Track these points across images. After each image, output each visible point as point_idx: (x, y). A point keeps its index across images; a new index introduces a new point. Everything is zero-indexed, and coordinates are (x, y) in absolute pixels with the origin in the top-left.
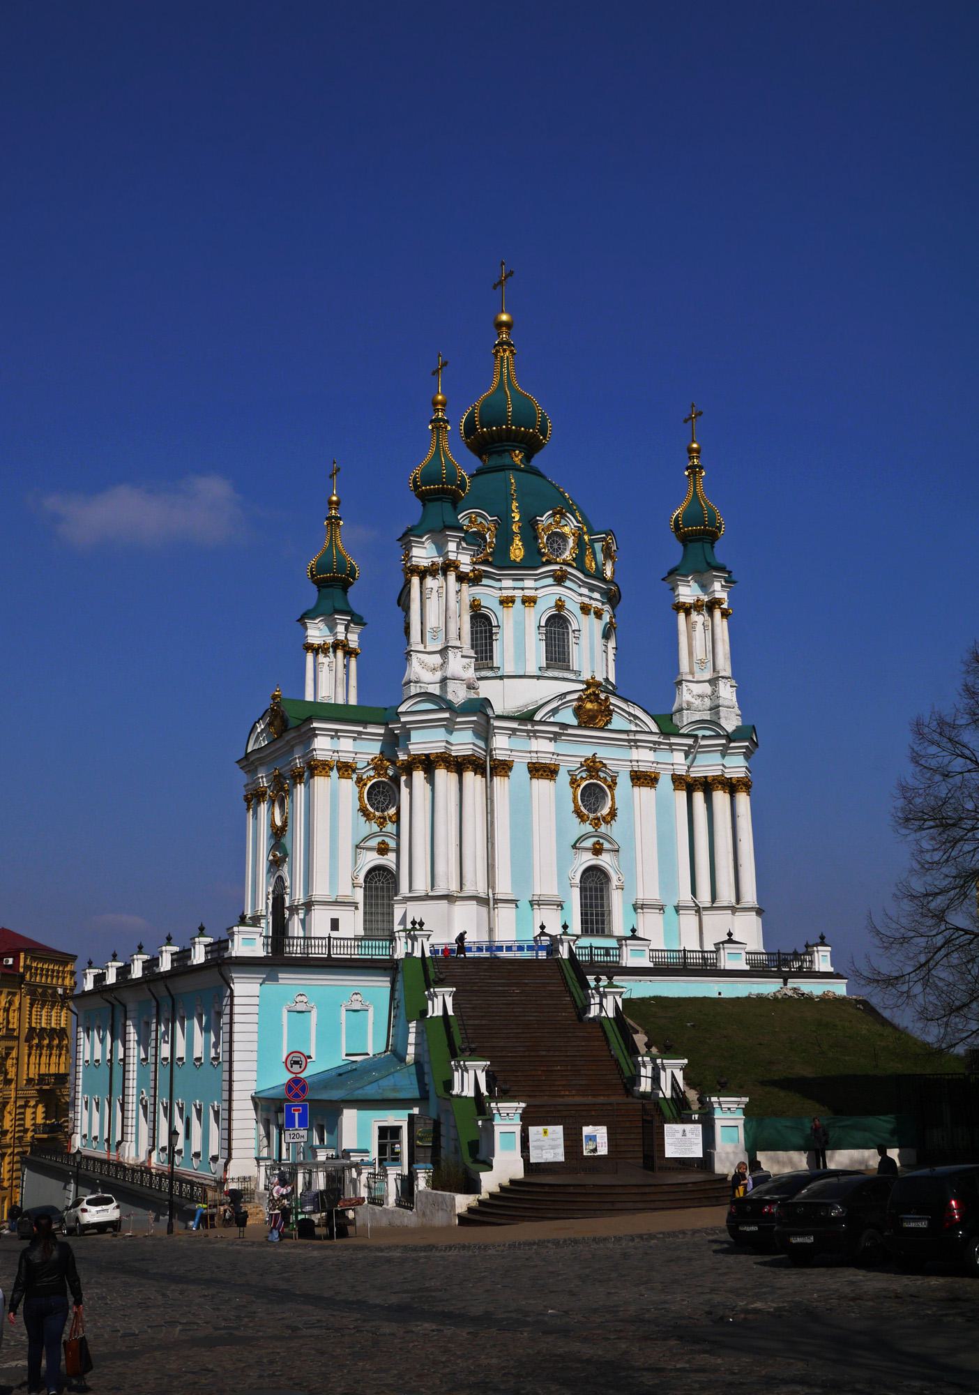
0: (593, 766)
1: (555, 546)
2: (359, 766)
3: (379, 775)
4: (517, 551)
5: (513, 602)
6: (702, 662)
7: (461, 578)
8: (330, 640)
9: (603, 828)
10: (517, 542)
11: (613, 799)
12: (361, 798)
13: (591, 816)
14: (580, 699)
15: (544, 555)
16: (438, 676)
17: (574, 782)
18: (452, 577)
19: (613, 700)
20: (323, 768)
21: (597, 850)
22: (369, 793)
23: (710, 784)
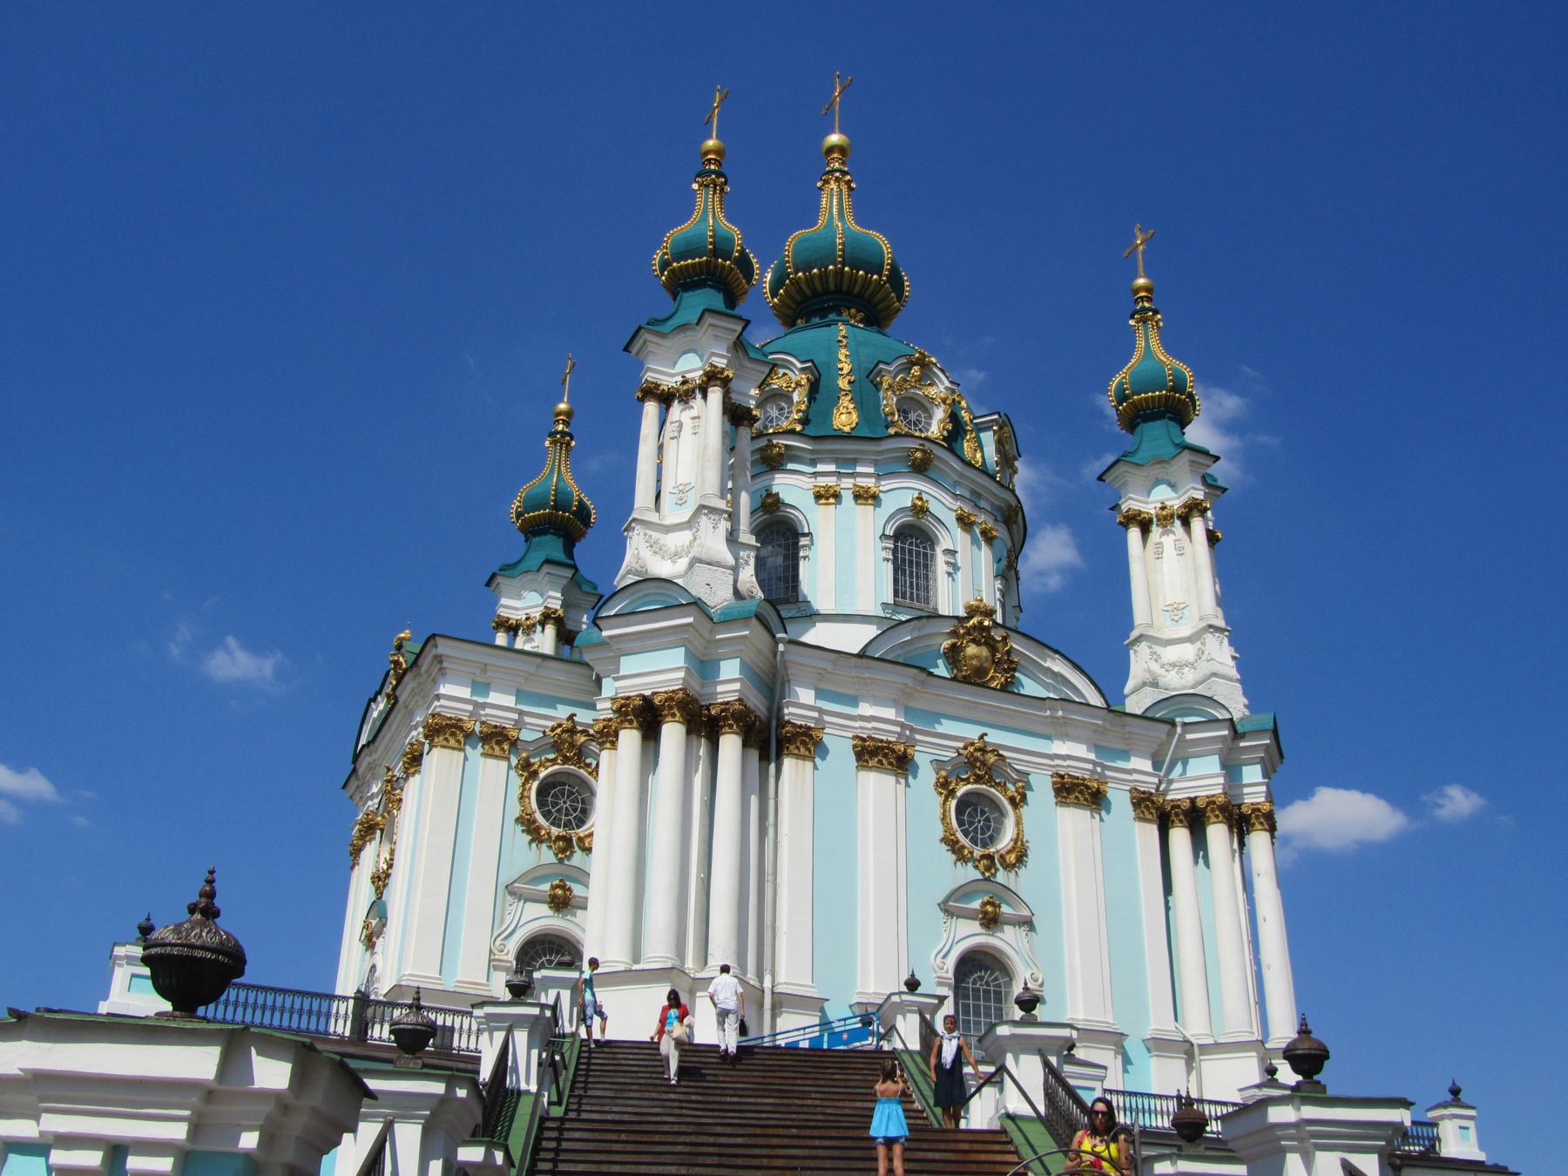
0: (979, 763)
1: (912, 416)
2: (526, 735)
3: (566, 760)
4: (845, 418)
5: (837, 496)
6: (1177, 610)
7: (736, 415)
8: (537, 614)
9: (1001, 876)
10: (845, 402)
11: (1018, 823)
12: (522, 797)
13: (978, 852)
14: (954, 633)
15: (893, 424)
16: (683, 563)
17: (945, 787)
18: (715, 394)
19: (1016, 644)
20: (444, 730)
21: (991, 921)
22: (541, 793)
23: (1203, 811)
